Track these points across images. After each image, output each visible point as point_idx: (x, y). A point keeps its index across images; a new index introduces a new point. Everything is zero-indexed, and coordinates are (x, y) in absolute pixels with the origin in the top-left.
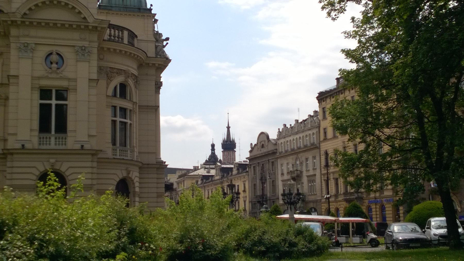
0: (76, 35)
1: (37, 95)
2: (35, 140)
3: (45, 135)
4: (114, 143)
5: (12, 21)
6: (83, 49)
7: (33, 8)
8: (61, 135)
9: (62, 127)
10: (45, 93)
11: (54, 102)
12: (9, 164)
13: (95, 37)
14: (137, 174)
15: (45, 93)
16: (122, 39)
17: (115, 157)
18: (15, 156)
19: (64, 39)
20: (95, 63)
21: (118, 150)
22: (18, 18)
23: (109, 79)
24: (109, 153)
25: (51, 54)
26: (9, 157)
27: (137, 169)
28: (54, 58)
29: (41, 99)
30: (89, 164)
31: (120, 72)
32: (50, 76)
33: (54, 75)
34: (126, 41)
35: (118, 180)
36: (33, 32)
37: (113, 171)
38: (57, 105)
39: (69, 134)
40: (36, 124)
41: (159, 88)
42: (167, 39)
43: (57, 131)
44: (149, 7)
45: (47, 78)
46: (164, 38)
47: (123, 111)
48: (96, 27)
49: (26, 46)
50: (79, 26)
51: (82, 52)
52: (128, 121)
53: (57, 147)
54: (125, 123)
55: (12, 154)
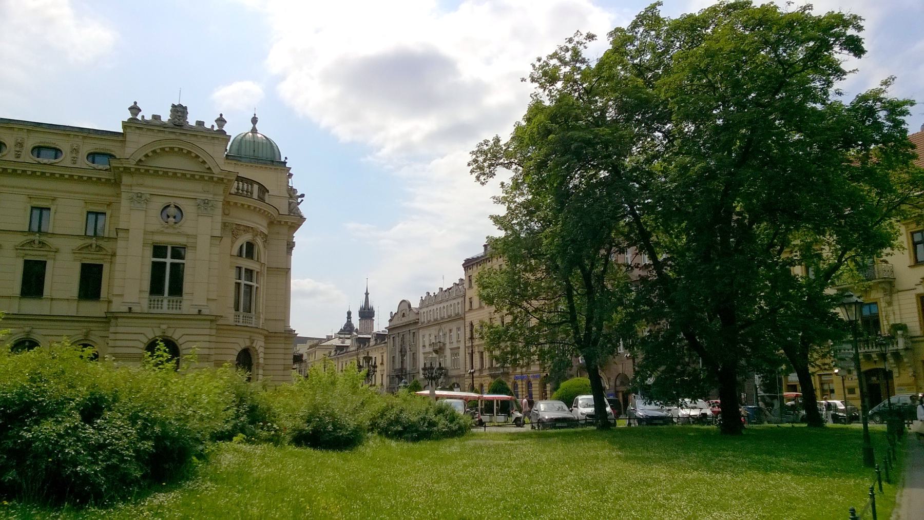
0: (198, 186)
1: (149, 252)
2: (145, 304)
3: (156, 297)
4: (237, 309)
5: (125, 168)
6: (206, 202)
7: (150, 154)
8: (175, 298)
9: (177, 289)
10: (159, 250)
11: (169, 260)
12: (112, 329)
13: (220, 189)
14: (263, 344)
15: (159, 250)
16: (252, 193)
18: (119, 320)
19: (184, 190)
20: (219, 218)
22: (132, 164)
23: (235, 236)
24: (231, 320)
25: (168, 206)
26: (113, 320)
27: (262, 338)
28: (172, 211)
29: (154, 256)
30: (207, 331)
31: (247, 229)
32: (166, 231)
33: (171, 230)
34: (255, 195)
35: (240, 350)
36: (148, 181)
37: (233, 340)
39: (185, 296)
41: (291, 248)
42: (302, 196)
43: (170, 294)
44: (283, 159)
45: (162, 233)
46: (299, 194)
47: (249, 272)
48: (222, 179)
49: (139, 196)
50: (202, 177)
51: (205, 205)
52: (254, 284)
53: (171, 311)
54: (251, 286)
55: (116, 318)
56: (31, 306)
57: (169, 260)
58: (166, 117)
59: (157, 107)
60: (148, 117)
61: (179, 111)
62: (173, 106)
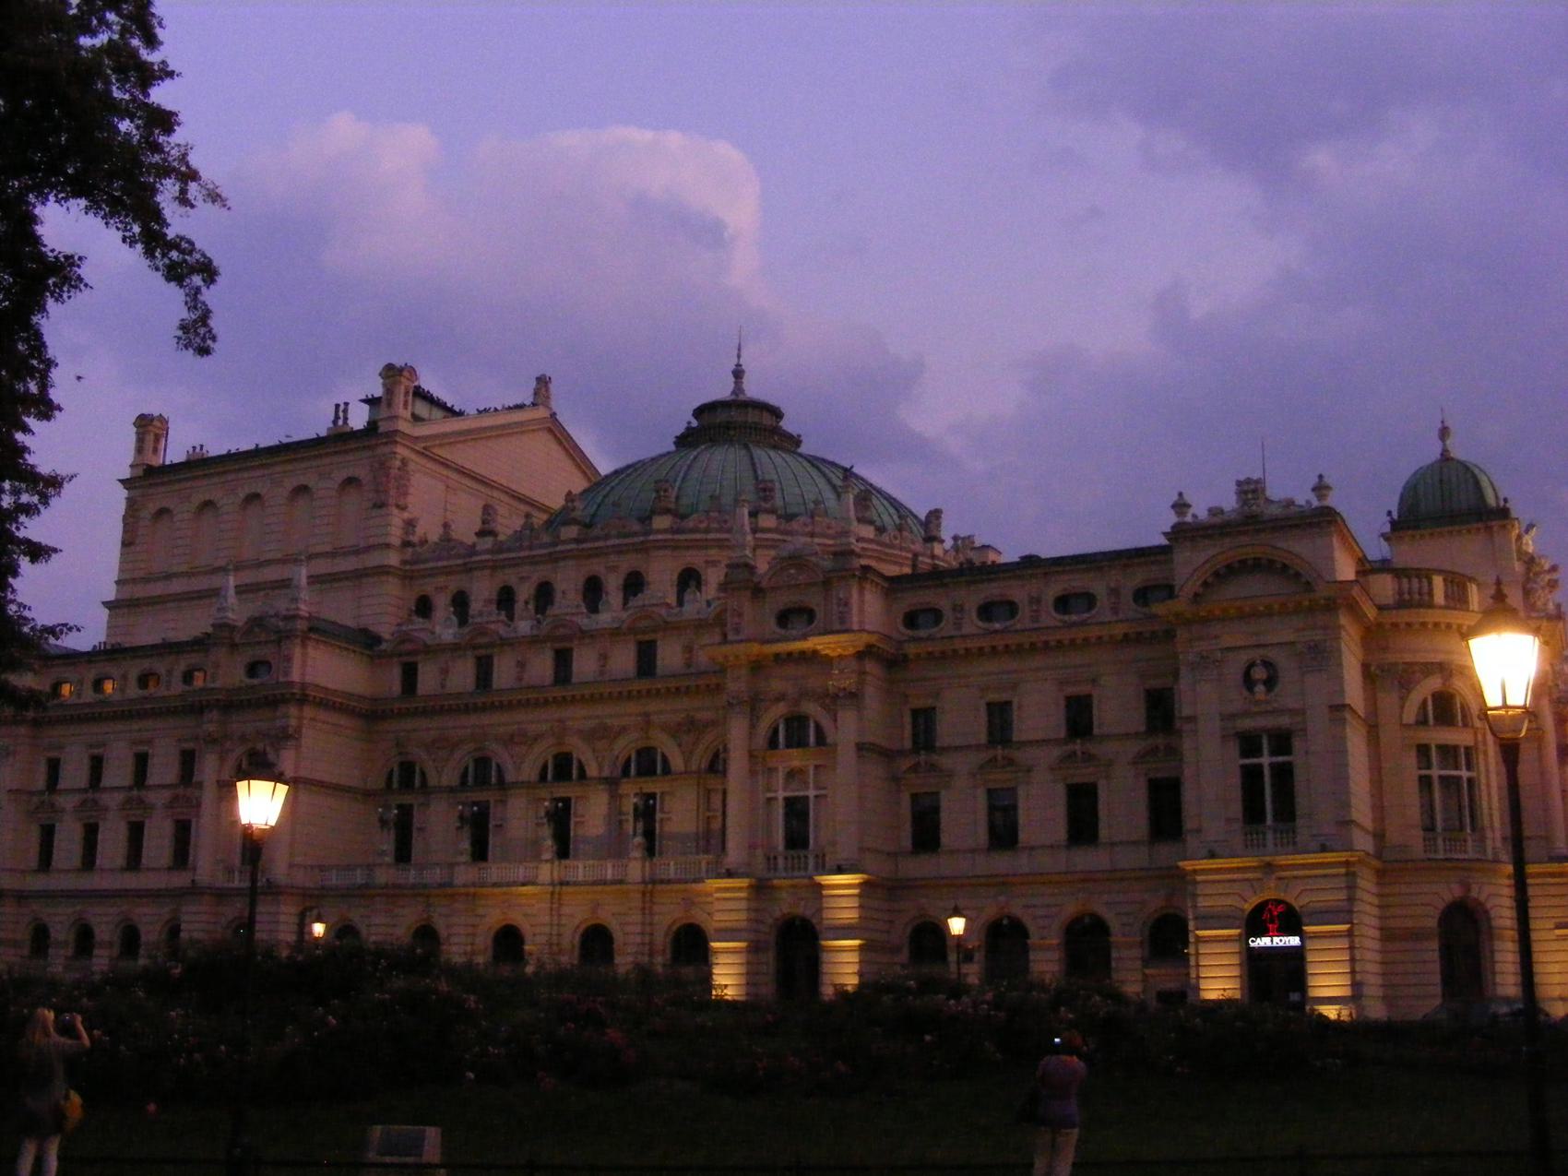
1: (1233, 749)
4: (1430, 828)
9: (1286, 811)
10: (1249, 744)
11: (1265, 760)
17: (1432, 856)
21: (1440, 841)
28: (1259, 673)
34: (1439, 597)
38: (1272, 765)
39: (1299, 822)
40: (1236, 809)
43: (1275, 818)
45: (1246, 714)
47: (1448, 752)
52: (1464, 773)
54: (1459, 778)
56: (1086, 859)
57: (1265, 760)
58: (1229, 502)
59: (1213, 495)
60: (1203, 515)
61: (1250, 490)
62: (1239, 483)
